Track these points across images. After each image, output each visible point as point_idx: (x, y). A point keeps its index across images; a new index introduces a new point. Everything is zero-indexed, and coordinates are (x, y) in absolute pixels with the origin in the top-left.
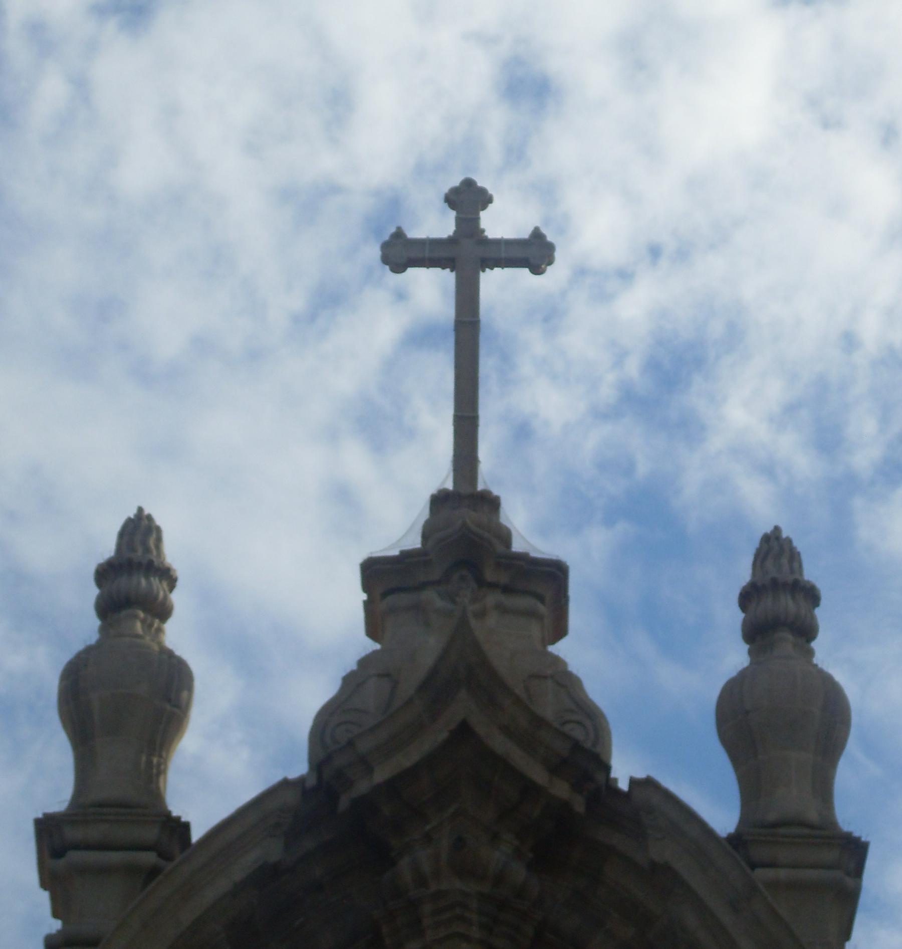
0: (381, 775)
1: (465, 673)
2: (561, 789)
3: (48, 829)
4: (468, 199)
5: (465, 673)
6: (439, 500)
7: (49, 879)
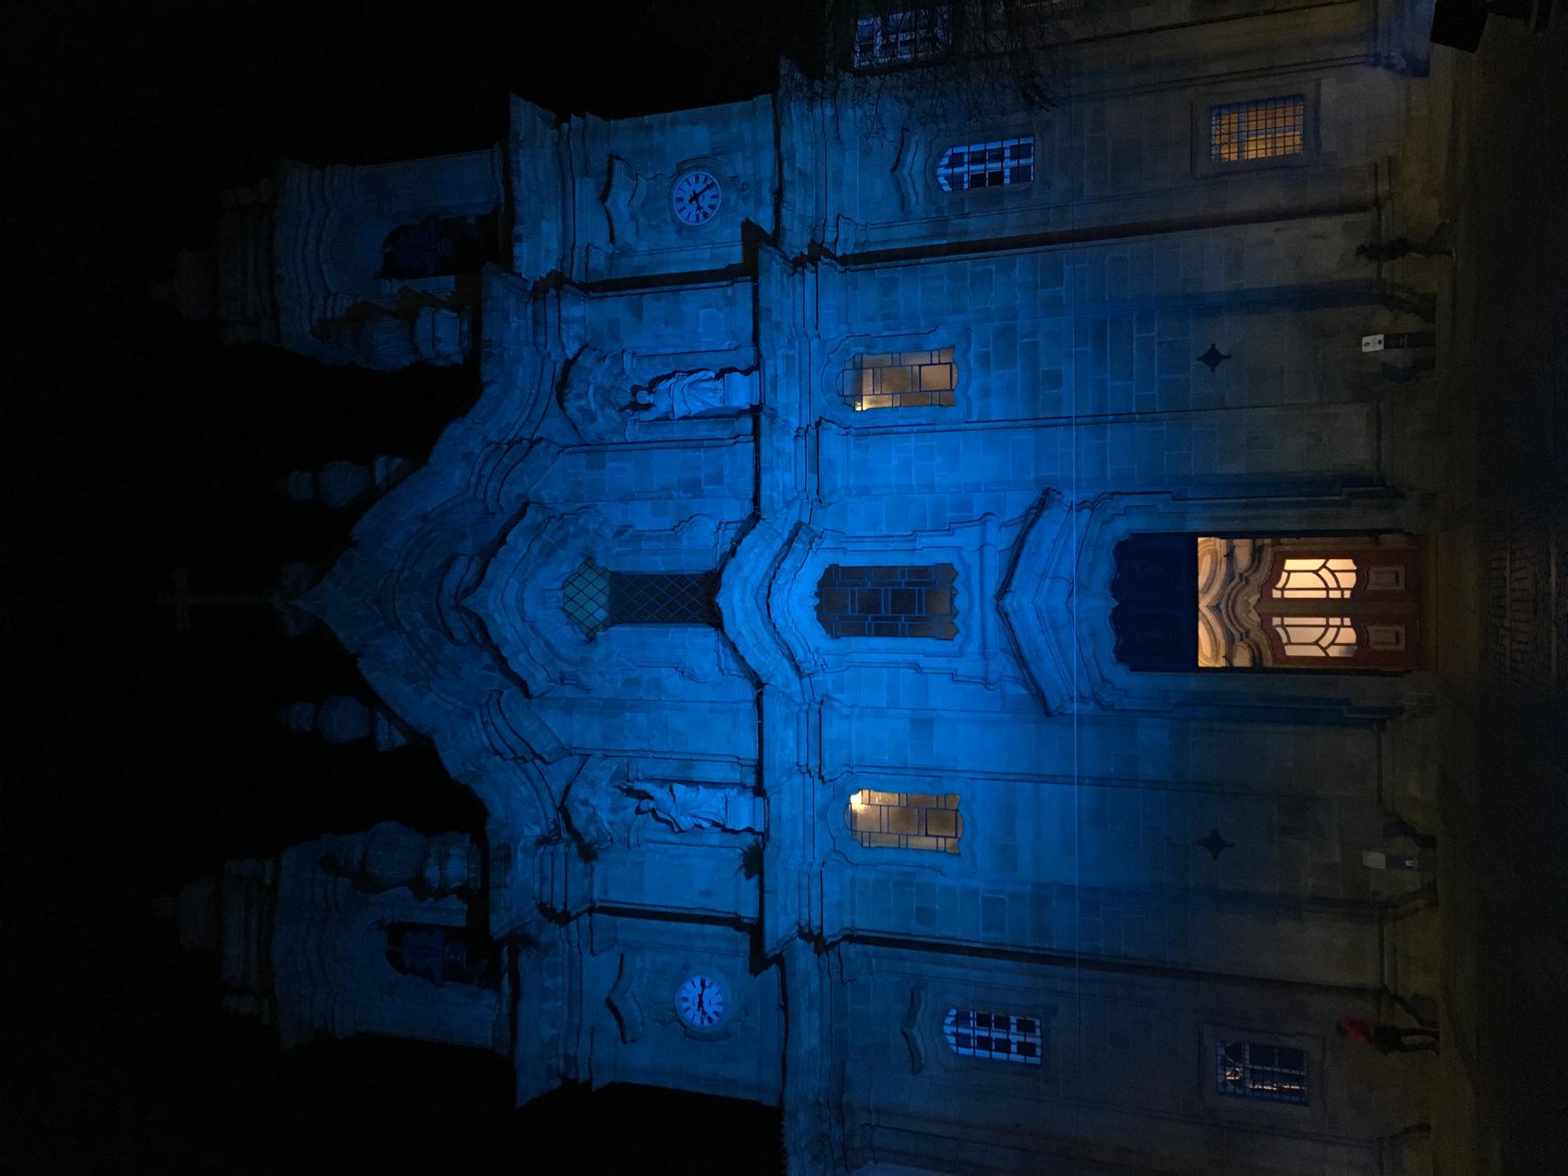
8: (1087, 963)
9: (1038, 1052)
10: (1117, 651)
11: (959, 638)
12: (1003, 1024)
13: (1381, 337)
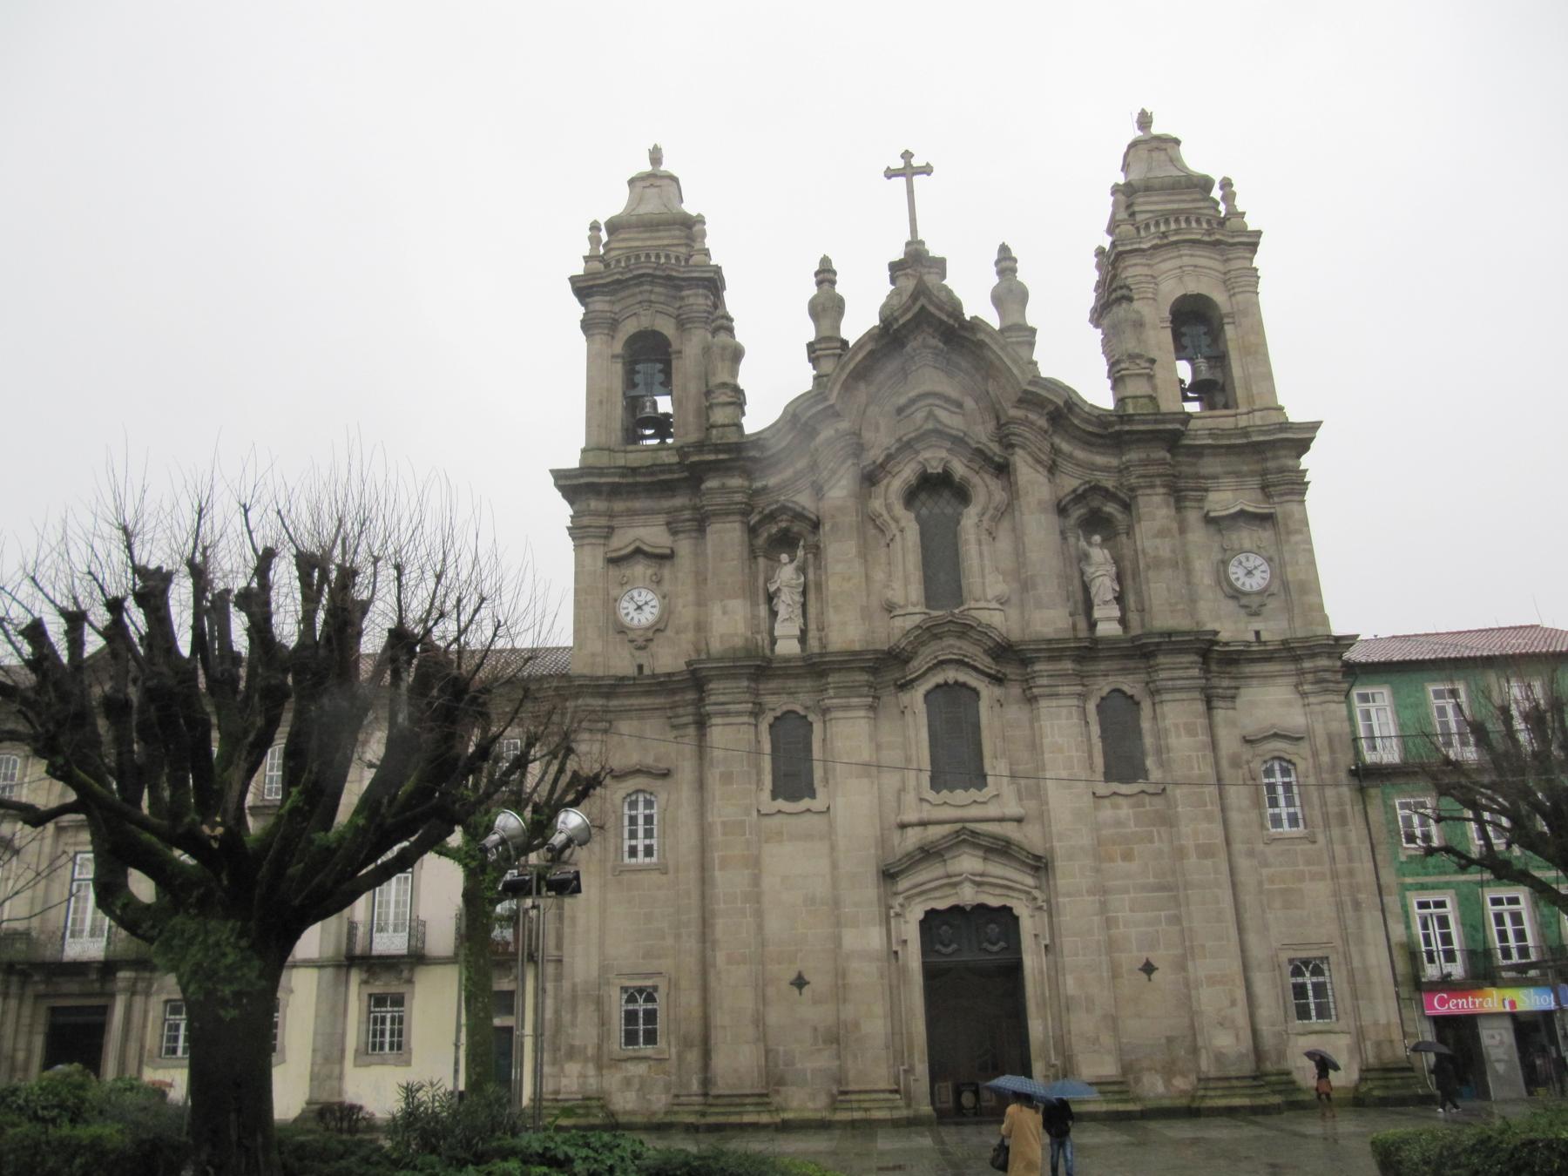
1: (921, 291)
2: (951, 322)
4: (907, 155)
5: (921, 291)
6: (908, 244)
7: (811, 360)
8: (703, 896)
9: (633, 860)
11: (930, 795)
12: (649, 834)
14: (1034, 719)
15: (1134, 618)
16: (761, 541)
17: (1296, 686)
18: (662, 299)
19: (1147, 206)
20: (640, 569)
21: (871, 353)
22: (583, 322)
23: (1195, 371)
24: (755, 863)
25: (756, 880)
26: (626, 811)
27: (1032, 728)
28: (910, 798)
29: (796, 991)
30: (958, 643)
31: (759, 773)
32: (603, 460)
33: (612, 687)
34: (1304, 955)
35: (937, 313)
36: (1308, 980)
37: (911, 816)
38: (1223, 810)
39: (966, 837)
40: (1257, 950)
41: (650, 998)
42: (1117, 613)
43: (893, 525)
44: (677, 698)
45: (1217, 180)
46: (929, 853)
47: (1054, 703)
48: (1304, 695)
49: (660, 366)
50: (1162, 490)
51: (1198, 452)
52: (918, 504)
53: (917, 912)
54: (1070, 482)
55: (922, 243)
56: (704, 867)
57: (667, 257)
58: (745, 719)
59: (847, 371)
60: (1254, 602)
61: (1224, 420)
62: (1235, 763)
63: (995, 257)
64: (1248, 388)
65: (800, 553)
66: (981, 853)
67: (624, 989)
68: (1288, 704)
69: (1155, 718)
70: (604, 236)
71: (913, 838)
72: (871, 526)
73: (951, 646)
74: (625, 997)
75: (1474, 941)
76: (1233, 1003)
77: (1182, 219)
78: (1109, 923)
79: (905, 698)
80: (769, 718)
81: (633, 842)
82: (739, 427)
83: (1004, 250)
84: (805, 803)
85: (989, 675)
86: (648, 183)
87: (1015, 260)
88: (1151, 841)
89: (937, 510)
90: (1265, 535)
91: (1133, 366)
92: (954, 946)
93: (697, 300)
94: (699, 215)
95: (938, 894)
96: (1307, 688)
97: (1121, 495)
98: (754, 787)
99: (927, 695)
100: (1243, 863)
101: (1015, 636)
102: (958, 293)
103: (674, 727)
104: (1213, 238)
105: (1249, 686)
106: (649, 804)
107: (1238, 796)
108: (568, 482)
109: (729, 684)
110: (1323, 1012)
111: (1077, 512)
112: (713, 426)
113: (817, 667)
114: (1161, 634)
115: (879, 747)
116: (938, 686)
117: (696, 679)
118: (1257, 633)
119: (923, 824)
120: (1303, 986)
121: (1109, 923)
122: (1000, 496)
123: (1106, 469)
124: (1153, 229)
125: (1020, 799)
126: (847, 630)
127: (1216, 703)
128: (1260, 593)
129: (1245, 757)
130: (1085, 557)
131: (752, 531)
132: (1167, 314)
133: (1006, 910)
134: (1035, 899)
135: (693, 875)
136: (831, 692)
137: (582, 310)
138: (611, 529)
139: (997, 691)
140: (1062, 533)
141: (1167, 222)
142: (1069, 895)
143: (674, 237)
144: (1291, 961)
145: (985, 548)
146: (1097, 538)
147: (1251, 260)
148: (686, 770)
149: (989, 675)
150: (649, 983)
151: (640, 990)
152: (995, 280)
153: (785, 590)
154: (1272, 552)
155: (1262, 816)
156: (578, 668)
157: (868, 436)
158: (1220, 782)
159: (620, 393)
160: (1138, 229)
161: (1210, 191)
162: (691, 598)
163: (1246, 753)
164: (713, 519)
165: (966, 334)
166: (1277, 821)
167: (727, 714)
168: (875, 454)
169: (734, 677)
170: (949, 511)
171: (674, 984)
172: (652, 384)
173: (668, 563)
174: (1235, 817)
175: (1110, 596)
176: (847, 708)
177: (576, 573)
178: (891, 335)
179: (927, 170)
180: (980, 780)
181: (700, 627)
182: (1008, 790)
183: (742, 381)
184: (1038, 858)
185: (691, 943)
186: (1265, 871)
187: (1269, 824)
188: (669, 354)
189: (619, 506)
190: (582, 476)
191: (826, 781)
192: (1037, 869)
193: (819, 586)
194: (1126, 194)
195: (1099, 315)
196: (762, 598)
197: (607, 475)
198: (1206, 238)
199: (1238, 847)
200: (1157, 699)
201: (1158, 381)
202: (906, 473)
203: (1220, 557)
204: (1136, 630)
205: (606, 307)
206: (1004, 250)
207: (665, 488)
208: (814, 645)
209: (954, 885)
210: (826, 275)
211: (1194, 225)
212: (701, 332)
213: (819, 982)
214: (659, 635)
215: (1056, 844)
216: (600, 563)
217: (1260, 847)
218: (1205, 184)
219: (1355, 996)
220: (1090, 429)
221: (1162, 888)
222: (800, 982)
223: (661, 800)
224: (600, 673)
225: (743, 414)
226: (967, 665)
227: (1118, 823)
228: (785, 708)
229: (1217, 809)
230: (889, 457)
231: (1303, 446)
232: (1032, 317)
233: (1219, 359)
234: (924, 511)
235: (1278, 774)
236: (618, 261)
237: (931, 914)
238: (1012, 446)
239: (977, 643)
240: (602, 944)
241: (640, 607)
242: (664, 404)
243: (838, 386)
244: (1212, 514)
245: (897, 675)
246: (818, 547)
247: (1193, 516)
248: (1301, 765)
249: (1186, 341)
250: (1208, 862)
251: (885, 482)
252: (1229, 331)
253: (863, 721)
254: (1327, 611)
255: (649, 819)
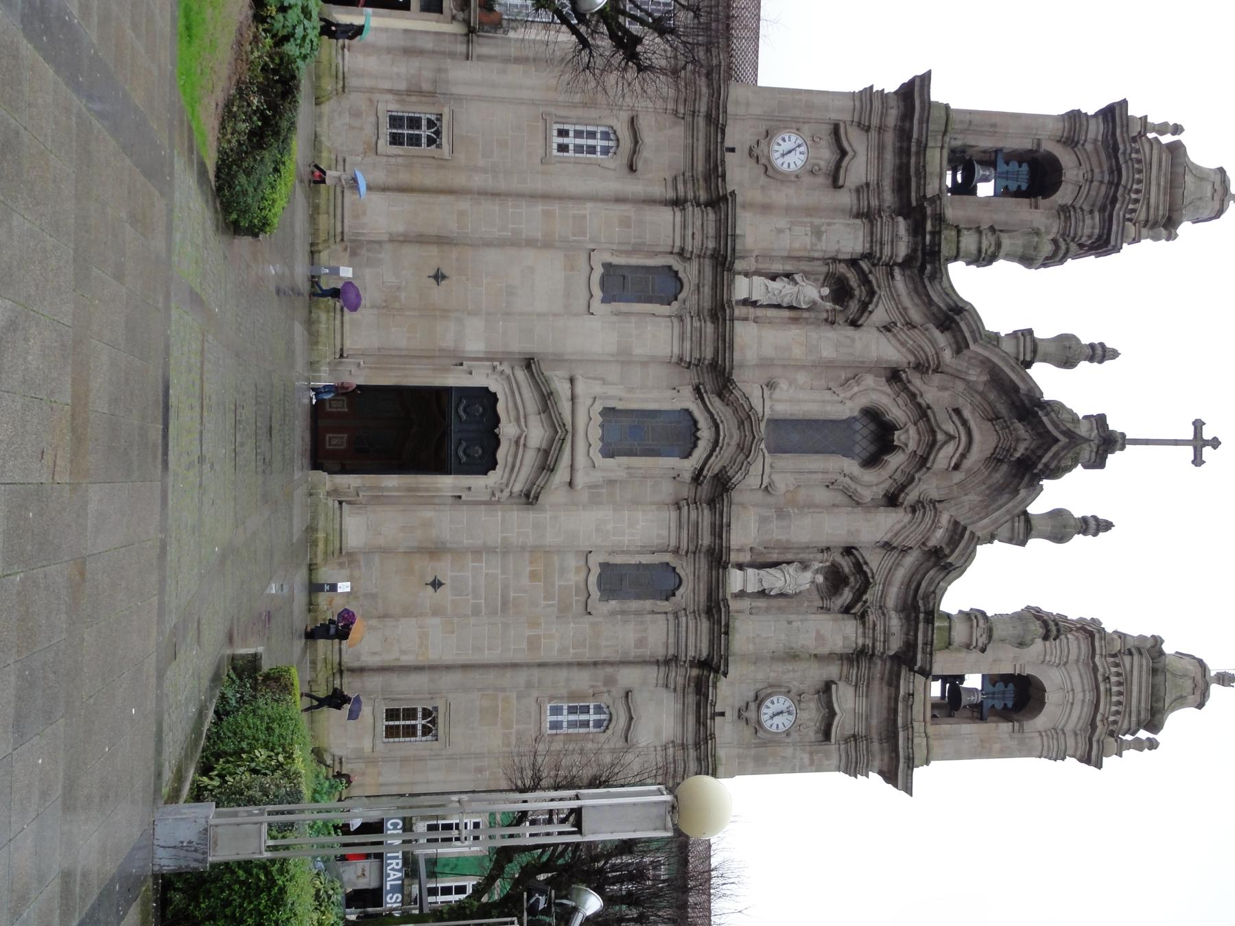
0: (1045, 419)
2: (1040, 466)
3: (1030, 332)
4: (1215, 443)
5: (1074, 439)
6: (1123, 435)
7: (1015, 332)
8: (520, 195)
9: (555, 133)
10: (496, 400)
11: (598, 407)
12: (579, 149)
13: (339, 590)
14: (661, 505)
15: (745, 604)
16: (842, 268)
17: (673, 742)
18: (1093, 193)
19: (1137, 668)
20: (826, 155)
21: (1016, 389)
22: (1079, 111)
23: (972, 691)
24: (546, 244)
25: (531, 243)
26: (600, 129)
27: (653, 504)
28: (598, 389)
29: (432, 273)
30: (734, 443)
31: (628, 253)
32: (936, 125)
33: (716, 122)
34: (440, 720)
35: (1050, 454)
36: (419, 722)
37: (580, 388)
38: (569, 664)
39: (560, 434)
40: (447, 680)
41: (431, 141)
42: (749, 591)
43: (849, 394)
44: (701, 182)
45: (1158, 737)
46: (547, 400)
47: (673, 525)
48: (665, 748)
49: (1024, 187)
50: (860, 642)
51: (893, 682)
52: (865, 421)
53: (495, 385)
54: (875, 561)
55: (1122, 449)
56: (546, 197)
57: (1136, 201)
58: (678, 244)
59: (1001, 364)
60: (751, 714)
61: (919, 710)
62: (610, 681)
63: (1100, 517)
64: (948, 736)
65: (829, 305)
66: (544, 446)
67: (440, 117)
68: (658, 733)
69: (653, 612)
70: (1166, 139)
71: (562, 388)
72: (850, 375)
73: (731, 437)
74: (433, 118)
75: (445, 865)
76: (403, 652)
77: (1121, 698)
78: (477, 552)
79: (687, 392)
80: (675, 268)
81: (571, 134)
82: (956, 258)
83: (1106, 526)
84: (598, 293)
85: (702, 469)
86: (1218, 186)
87: (1095, 535)
88: (545, 598)
89: (858, 437)
90: (811, 733)
91: (980, 631)
92: (464, 417)
93: (1090, 226)
94: (1176, 235)
95: (510, 404)
96: (671, 751)
97: (859, 605)
98: (615, 247)
99: (688, 412)
100: (522, 677)
101: (736, 496)
102: (1067, 477)
103: (675, 178)
104: (1099, 723)
105: (676, 702)
106: (606, 150)
107: (582, 680)
108: (917, 89)
109: (711, 231)
110: (391, 732)
111: (846, 565)
112: (959, 232)
113: (720, 312)
114: (727, 625)
115: (644, 364)
116: (695, 422)
117: (719, 201)
118: (722, 714)
119: (573, 398)
120: (415, 718)
121: (477, 552)
122: (867, 494)
123: (883, 595)
124: (1113, 670)
125: (589, 487)
126: (753, 341)
127: (662, 669)
128: (759, 722)
129: (613, 689)
130: (805, 566)
131: (853, 263)
132: (1028, 671)
133: (493, 465)
134: (502, 491)
135: (539, 185)
136: (697, 324)
137: (1091, 112)
138: (867, 129)
139: (687, 476)
140: (828, 549)
141: (1119, 684)
142: (503, 521)
143: (1157, 208)
144: (436, 709)
145: (820, 476)
146: (820, 579)
147: (1073, 756)
148: (634, 187)
149: (702, 469)
150: (444, 140)
151: (438, 133)
152: (1078, 514)
153: (796, 289)
154: (795, 736)
155: (561, 698)
156: (736, 93)
157: (937, 378)
158: (595, 664)
159: (1000, 145)
160: (1115, 656)
161: (1147, 728)
162: (795, 202)
163: (618, 692)
164: (868, 227)
165: (1027, 478)
166: (556, 711)
167: (684, 227)
168: (917, 382)
169: (718, 237)
170: (857, 449)
171: (442, 163)
172: (1007, 179)
173: (830, 181)
174: (563, 674)
175: (766, 586)
176: (682, 338)
177: (828, 92)
178: (1030, 408)
179: (1198, 461)
180: (608, 453)
181: (766, 208)
182: (597, 476)
183: (1001, 265)
184: (536, 498)
185: (478, 181)
186: (514, 695)
187: (553, 704)
188: (1035, 196)
189: (890, 138)
190: (922, 102)
191: (618, 314)
192: (527, 496)
193: (795, 320)
194: (1152, 648)
195: (1035, 615)
196: (789, 268)
197: (920, 129)
198: (1099, 717)
199: (536, 673)
200: (671, 617)
201: (963, 654)
202: (897, 411)
203: (794, 691)
204: (734, 605)
205: (1091, 136)
206: (1106, 526)
207: (901, 185)
208: (739, 311)
209: (518, 420)
210: (1099, 353)
211: (1114, 708)
212: (1055, 230)
213: (437, 293)
214: (763, 170)
215: (548, 515)
216: (835, 116)
217: (535, 694)
218: (1154, 724)
219: (404, 760)
220: (924, 584)
221: (505, 603)
222: (439, 277)
223: (609, 161)
224: (730, 109)
225: (968, 264)
226: (713, 450)
227: (563, 571)
228: (685, 280)
229: (569, 657)
230: (913, 396)
231: (890, 776)
232: (1038, 546)
233: (979, 712)
234: (858, 426)
235: (597, 717)
236: (1138, 151)
237: (493, 398)
238: (914, 510)
239: (733, 461)
240: (480, 98)
241: (790, 153)
242: (985, 189)
243: (986, 353)
244: (834, 687)
245: (708, 387)
246: (833, 323)
247: (833, 671)
248: (603, 737)
249: (1000, 686)
250: (524, 645)
251: (889, 390)
252: (1005, 727)
253: (669, 350)
254: (738, 778)
255: (592, 150)
